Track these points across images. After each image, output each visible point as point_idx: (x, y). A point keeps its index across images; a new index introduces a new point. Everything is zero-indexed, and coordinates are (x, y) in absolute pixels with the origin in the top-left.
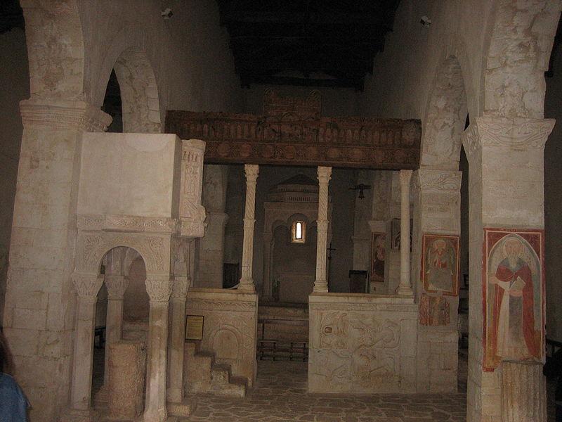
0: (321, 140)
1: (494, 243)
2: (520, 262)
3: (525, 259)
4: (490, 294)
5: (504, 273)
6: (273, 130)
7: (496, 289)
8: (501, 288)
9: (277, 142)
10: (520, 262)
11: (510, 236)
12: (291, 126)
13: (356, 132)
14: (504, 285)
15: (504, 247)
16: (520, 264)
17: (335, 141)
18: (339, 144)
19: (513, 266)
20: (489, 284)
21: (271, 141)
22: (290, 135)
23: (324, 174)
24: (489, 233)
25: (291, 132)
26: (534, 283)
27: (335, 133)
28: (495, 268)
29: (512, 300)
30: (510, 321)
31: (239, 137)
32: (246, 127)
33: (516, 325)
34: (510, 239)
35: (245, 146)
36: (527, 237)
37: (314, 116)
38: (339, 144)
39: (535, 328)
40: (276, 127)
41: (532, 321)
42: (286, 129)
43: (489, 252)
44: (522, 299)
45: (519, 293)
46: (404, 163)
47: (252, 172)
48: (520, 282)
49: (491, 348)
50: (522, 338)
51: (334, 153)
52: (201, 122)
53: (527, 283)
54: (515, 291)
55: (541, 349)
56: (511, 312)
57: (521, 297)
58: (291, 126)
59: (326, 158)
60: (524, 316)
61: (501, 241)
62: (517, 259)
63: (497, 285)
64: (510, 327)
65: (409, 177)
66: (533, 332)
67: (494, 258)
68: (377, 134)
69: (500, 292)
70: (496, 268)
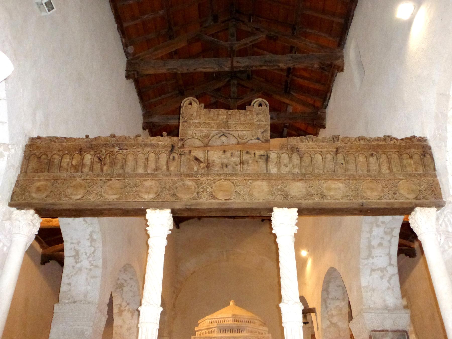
0: (273, 170)
6: (197, 159)
9: (202, 175)
12: (224, 152)
13: (329, 157)
17: (296, 170)
18: (304, 175)
21: (192, 176)
22: (224, 166)
23: (285, 222)
25: (225, 161)
27: (296, 159)
31: (141, 171)
32: (152, 156)
35: (149, 183)
37: (259, 135)
38: (304, 175)
40: (200, 154)
42: (216, 156)
46: (416, 198)
47: (160, 223)
51: (297, 189)
52: (81, 150)
58: (224, 152)
59: (286, 196)
65: (434, 218)
68: (361, 159)
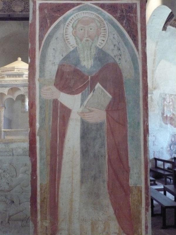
1: (51, 23)
2: (101, 56)
3: (112, 53)
4: (43, 120)
5: (70, 79)
7: (55, 110)
8: (63, 106)
10: (101, 56)
11: (79, 10)
14: (71, 101)
15: (70, 29)
16: (100, 60)
19: (87, 64)
20: (43, 102)
24: (40, 4)
26: (128, 96)
28: (52, 70)
29: (87, 131)
30: (83, 170)
33: (95, 178)
34: (82, 15)
36: (112, 9)
39: (132, 182)
41: (127, 170)
43: (41, 38)
44: (105, 127)
45: (99, 116)
48: (101, 95)
49: (47, 224)
50: (106, 201)
53: (114, 95)
54: (91, 111)
55: (143, 222)
56: (85, 152)
57: (101, 124)
60: (109, 160)
61: (65, 19)
62: (94, 52)
63: (56, 102)
64: (82, 182)
66: (126, 190)
67: (50, 52)
69: (62, 115)
70: (56, 68)
